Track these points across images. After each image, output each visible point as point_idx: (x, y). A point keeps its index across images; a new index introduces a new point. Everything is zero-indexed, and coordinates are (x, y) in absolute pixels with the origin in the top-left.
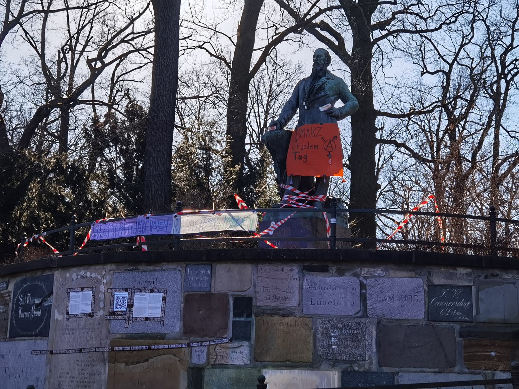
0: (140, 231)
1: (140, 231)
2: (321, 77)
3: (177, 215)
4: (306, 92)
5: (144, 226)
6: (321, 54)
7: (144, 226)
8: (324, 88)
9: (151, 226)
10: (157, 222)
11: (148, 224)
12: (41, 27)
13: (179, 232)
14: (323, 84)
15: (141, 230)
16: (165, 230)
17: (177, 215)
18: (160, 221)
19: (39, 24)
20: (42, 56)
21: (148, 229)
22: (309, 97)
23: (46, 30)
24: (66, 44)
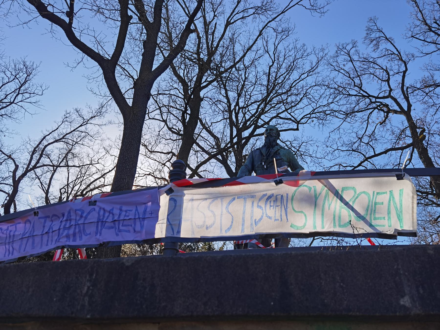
0: (68, 236)
1: (68, 236)
2: (275, 146)
3: (175, 188)
4: (264, 154)
5: (81, 222)
6: (274, 129)
7: (81, 222)
8: (279, 153)
9: (101, 222)
10: (116, 212)
11: (93, 217)
12: (50, 177)
13: (179, 232)
14: (278, 150)
15: (71, 232)
16: (138, 228)
17: (175, 188)
18: (124, 208)
19: (49, 175)
20: (47, 193)
21: (92, 229)
22: (267, 159)
23: (53, 180)
24: (63, 188)
